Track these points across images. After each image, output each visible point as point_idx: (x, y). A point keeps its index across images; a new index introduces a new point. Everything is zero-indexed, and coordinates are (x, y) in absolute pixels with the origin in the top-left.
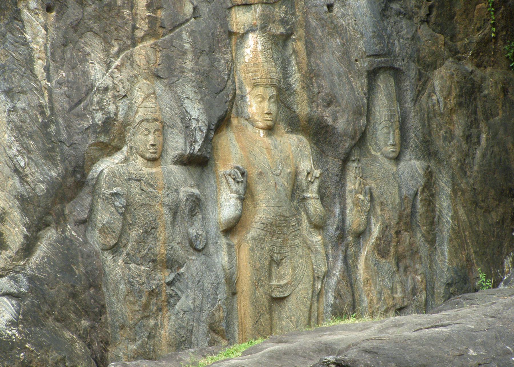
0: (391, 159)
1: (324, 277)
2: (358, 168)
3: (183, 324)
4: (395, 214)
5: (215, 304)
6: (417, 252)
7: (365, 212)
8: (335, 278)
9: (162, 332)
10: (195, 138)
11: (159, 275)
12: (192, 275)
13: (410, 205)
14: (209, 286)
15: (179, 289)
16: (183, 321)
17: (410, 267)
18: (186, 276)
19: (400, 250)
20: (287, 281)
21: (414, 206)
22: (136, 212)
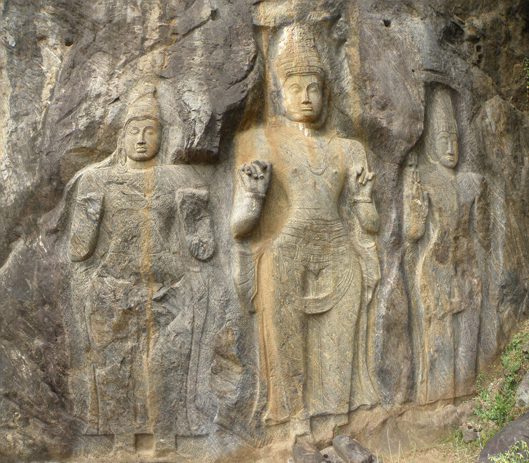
0: (449, 168)
1: (376, 286)
2: (415, 173)
3: (175, 348)
4: (453, 220)
5: (222, 325)
6: (474, 257)
7: (423, 218)
8: (389, 287)
9: (144, 357)
10: (194, 131)
11: (144, 290)
12: (192, 290)
13: (468, 212)
14: (216, 303)
15: (174, 306)
16: (174, 345)
17: (467, 270)
18: (182, 292)
19: (458, 255)
20: (327, 294)
21: (471, 214)
22: (114, 218)
